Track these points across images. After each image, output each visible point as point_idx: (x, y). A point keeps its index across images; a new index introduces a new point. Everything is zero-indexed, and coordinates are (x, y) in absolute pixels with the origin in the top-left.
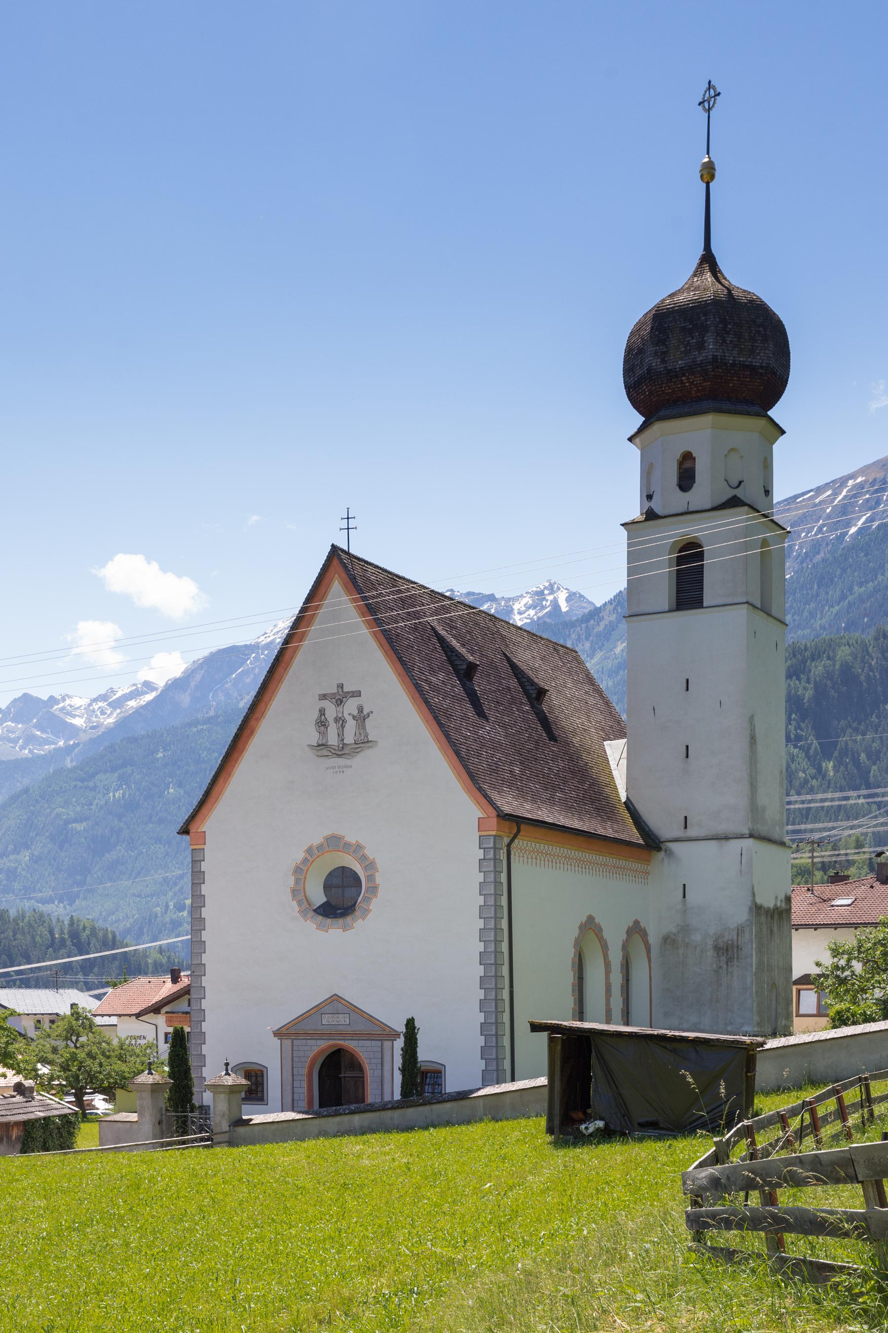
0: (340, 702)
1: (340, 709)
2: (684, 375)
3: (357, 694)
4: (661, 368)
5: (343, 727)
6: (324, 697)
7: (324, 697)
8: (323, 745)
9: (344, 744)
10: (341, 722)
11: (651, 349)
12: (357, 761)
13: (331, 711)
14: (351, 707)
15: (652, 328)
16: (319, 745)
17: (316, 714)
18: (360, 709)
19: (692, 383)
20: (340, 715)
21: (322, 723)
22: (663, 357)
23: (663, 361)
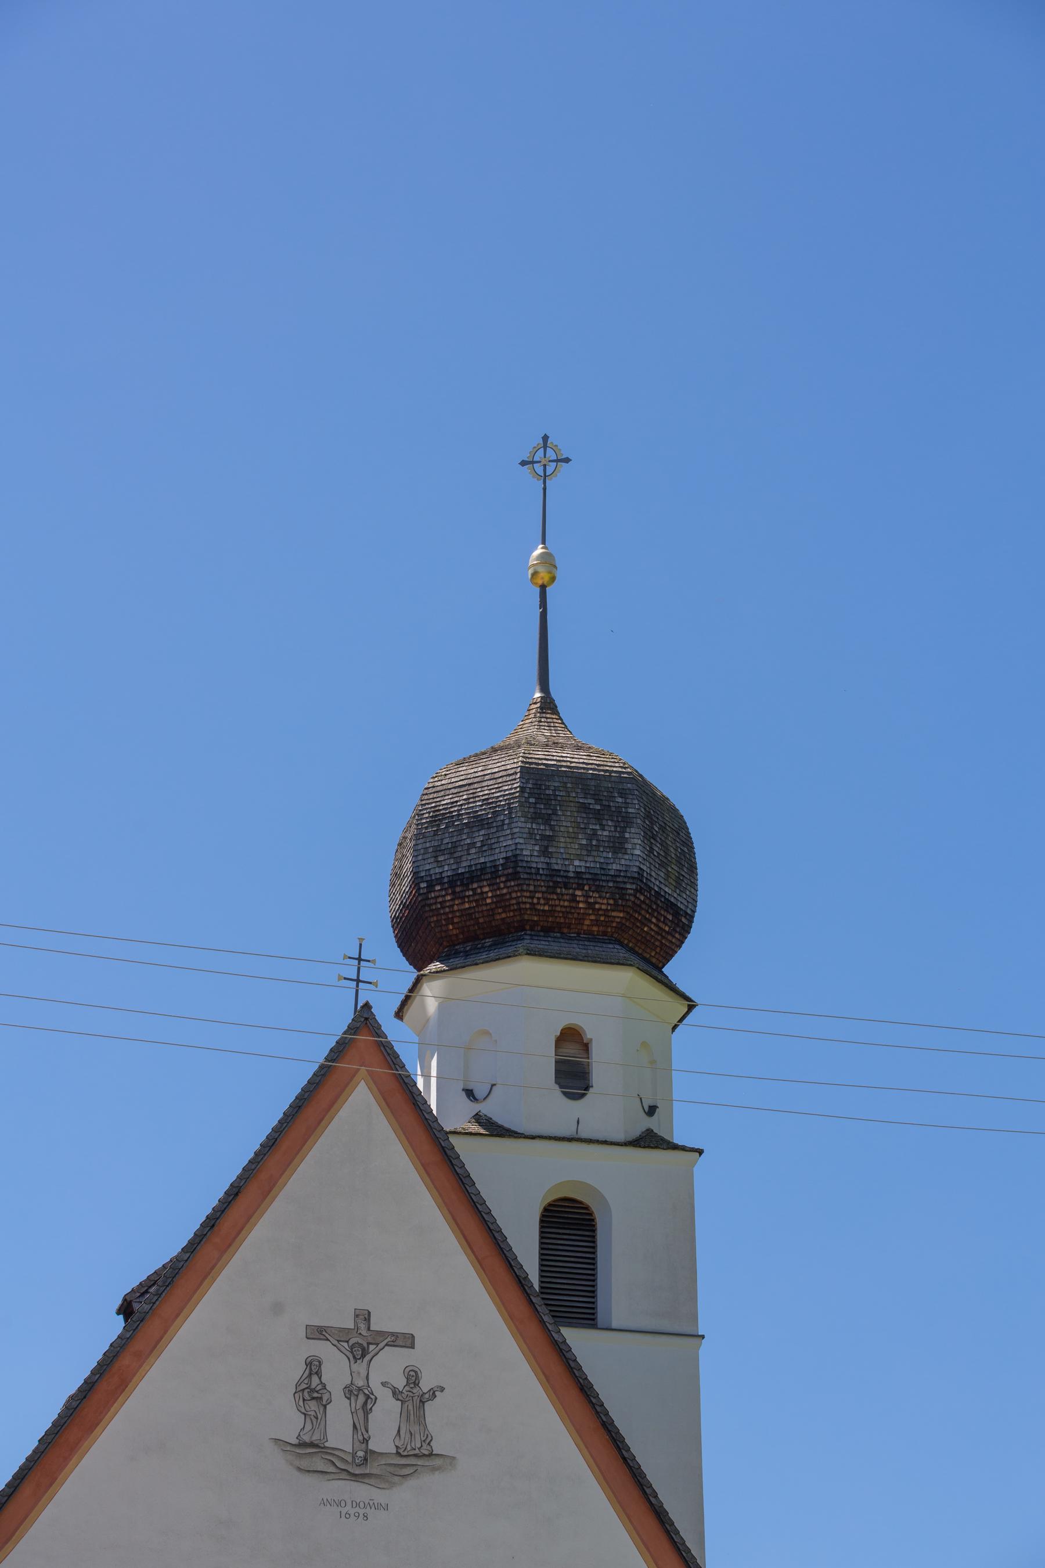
0: (360, 1352)
1: (360, 1367)
2: (580, 887)
3: (408, 1341)
4: (540, 862)
5: (366, 1412)
6: (318, 1333)
7: (318, 1333)
8: (312, 1445)
9: (370, 1455)
10: (361, 1399)
11: (521, 825)
12: (403, 1496)
13: (337, 1370)
14: (387, 1368)
15: (522, 789)
16: (303, 1445)
17: (298, 1371)
18: (413, 1378)
19: (591, 906)
20: (360, 1383)
21: (311, 1392)
22: (546, 844)
23: (545, 852)
